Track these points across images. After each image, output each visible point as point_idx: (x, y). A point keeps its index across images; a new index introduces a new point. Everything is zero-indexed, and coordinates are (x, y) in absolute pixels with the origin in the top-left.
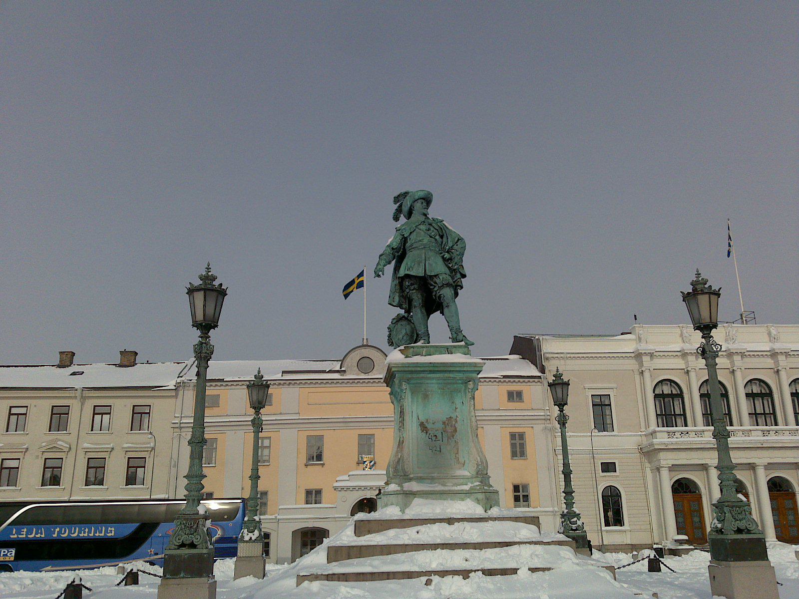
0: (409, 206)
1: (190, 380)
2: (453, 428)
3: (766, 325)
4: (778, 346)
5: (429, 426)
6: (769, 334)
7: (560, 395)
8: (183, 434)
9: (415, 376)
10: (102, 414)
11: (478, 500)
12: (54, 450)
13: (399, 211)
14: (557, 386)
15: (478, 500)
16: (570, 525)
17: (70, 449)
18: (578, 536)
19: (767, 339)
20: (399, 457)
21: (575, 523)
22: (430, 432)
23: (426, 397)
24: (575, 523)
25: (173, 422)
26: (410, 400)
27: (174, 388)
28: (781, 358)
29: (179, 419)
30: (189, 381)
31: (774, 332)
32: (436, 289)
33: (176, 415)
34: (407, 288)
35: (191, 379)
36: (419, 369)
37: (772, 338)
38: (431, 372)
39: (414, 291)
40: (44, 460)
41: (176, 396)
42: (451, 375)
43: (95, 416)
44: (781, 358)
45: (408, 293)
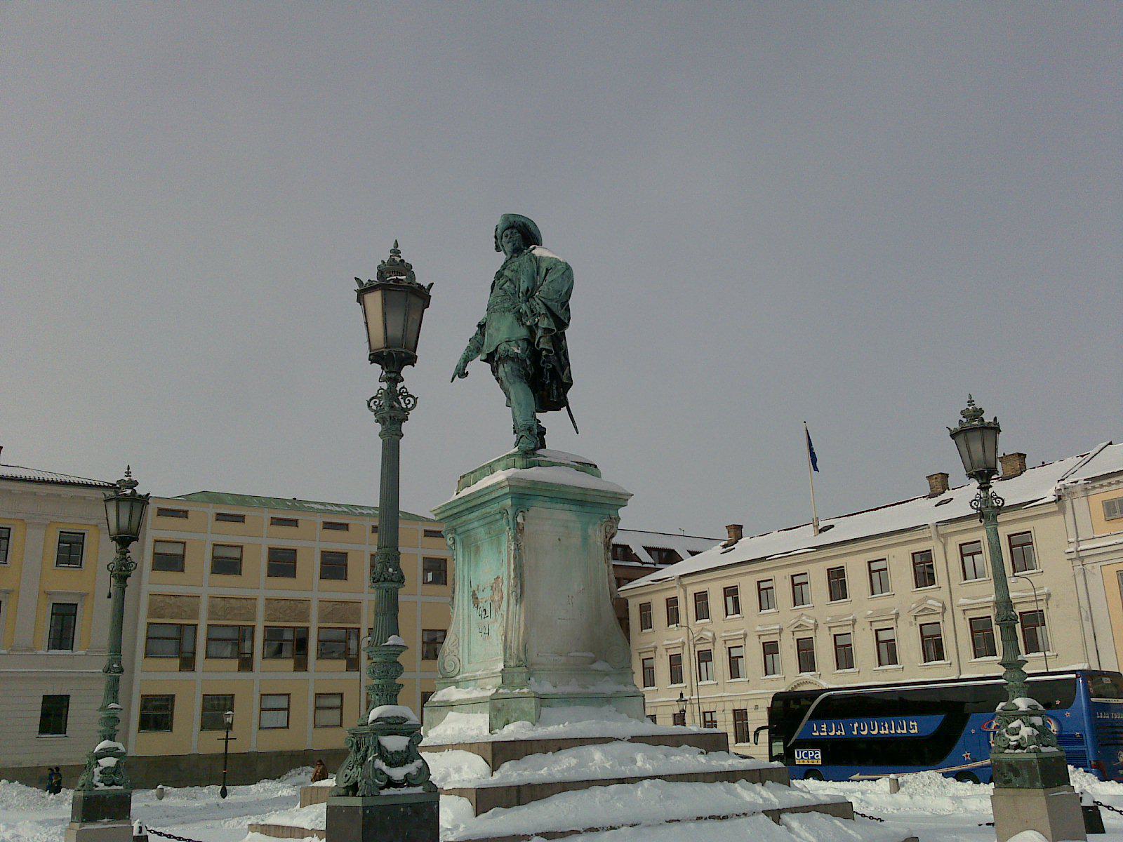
1: (1076, 482)
2: (500, 594)
5: (479, 595)
8: (1089, 567)
9: (459, 521)
10: (972, 554)
12: (926, 612)
14: (970, 435)
16: (1006, 735)
17: (944, 608)
18: (1018, 761)
21: (1016, 732)
22: (480, 605)
23: (478, 548)
24: (1016, 732)
25: (1066, 551)
26: (461, 559)
27: (1054, 499)
29: (1075, 545)
30: (1074, 484)
33: (1070, 540)
35: (1075, 480)
36: (455, 511)
38: (471, 510)
40: (968, 621)
41: (1062, 511)
42: (488, 509)
43: (965, 558)
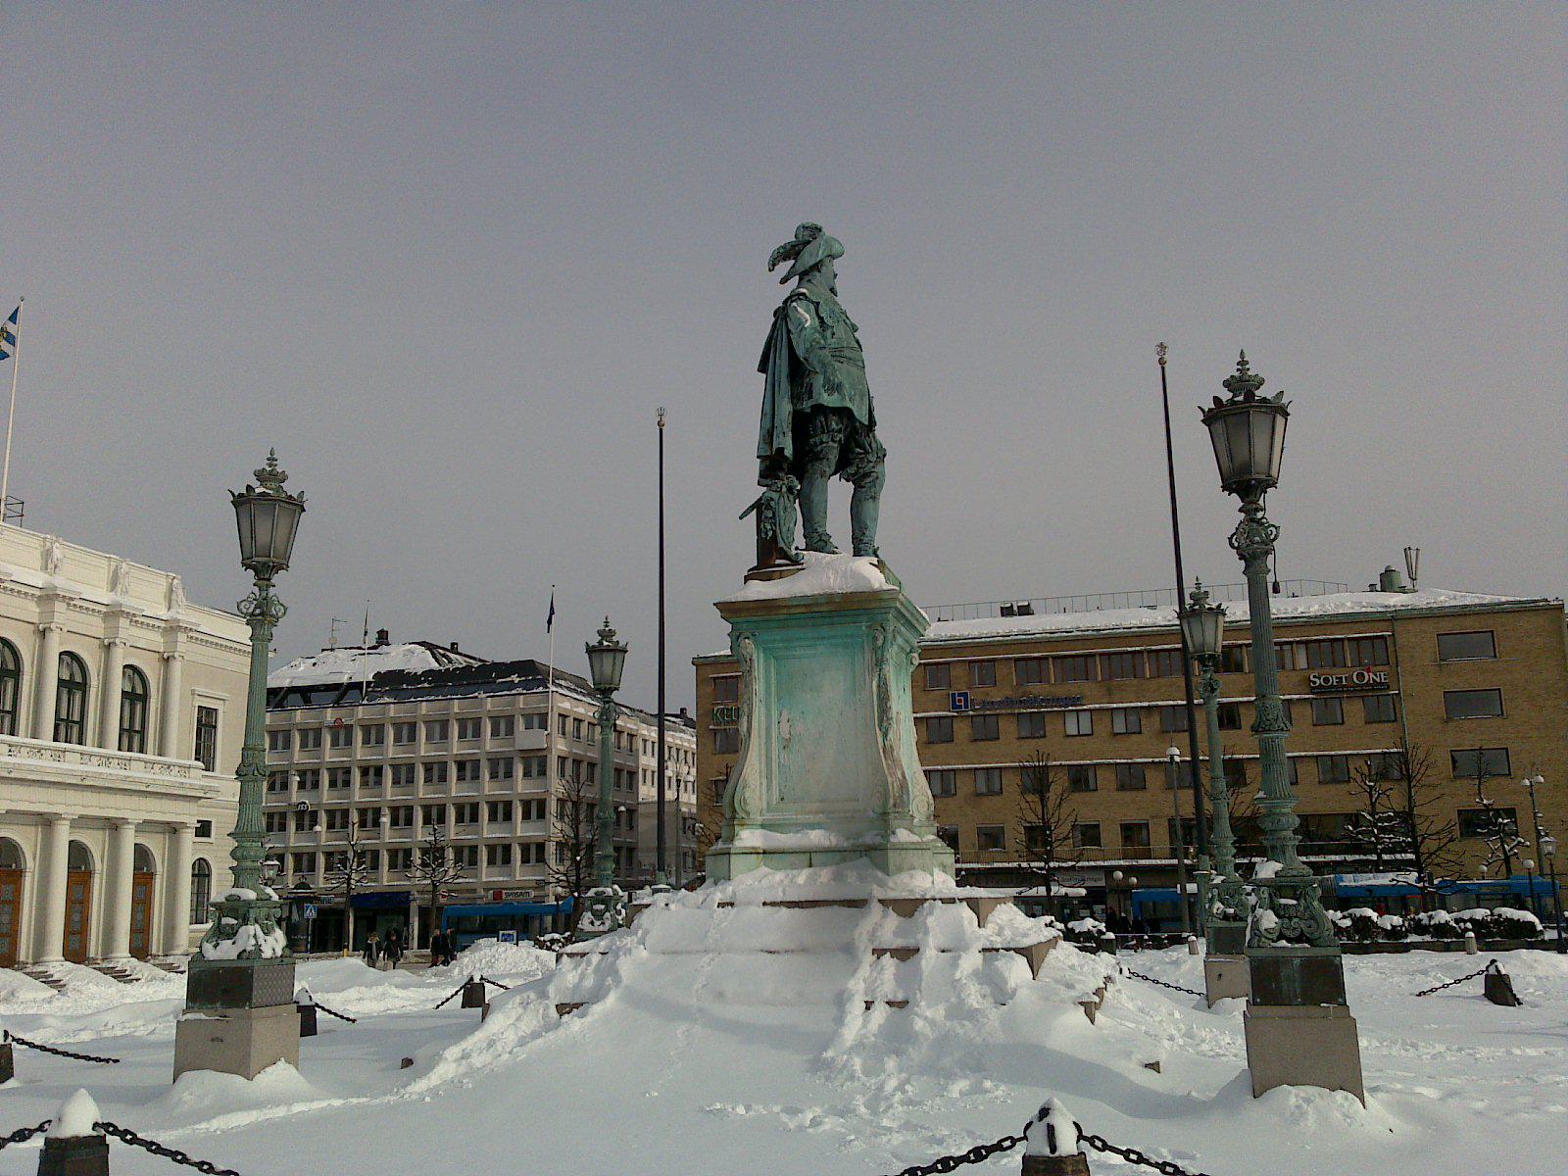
0: (819, 259)
3: (43, 536)
4: (60, 581)
6: (47, 555)
7: (608, 670)
11: (945, 867)
13: (791, 252)
15: (945, 867)
19: (38, 564)
20: (900, 776)
28: (60, 606)
31: (57, 553)
32: (870, 457)
34: (823, 433)
37: (47, 561)
39: (836, 445)
44: (60, 606)
45: (822, 443)
